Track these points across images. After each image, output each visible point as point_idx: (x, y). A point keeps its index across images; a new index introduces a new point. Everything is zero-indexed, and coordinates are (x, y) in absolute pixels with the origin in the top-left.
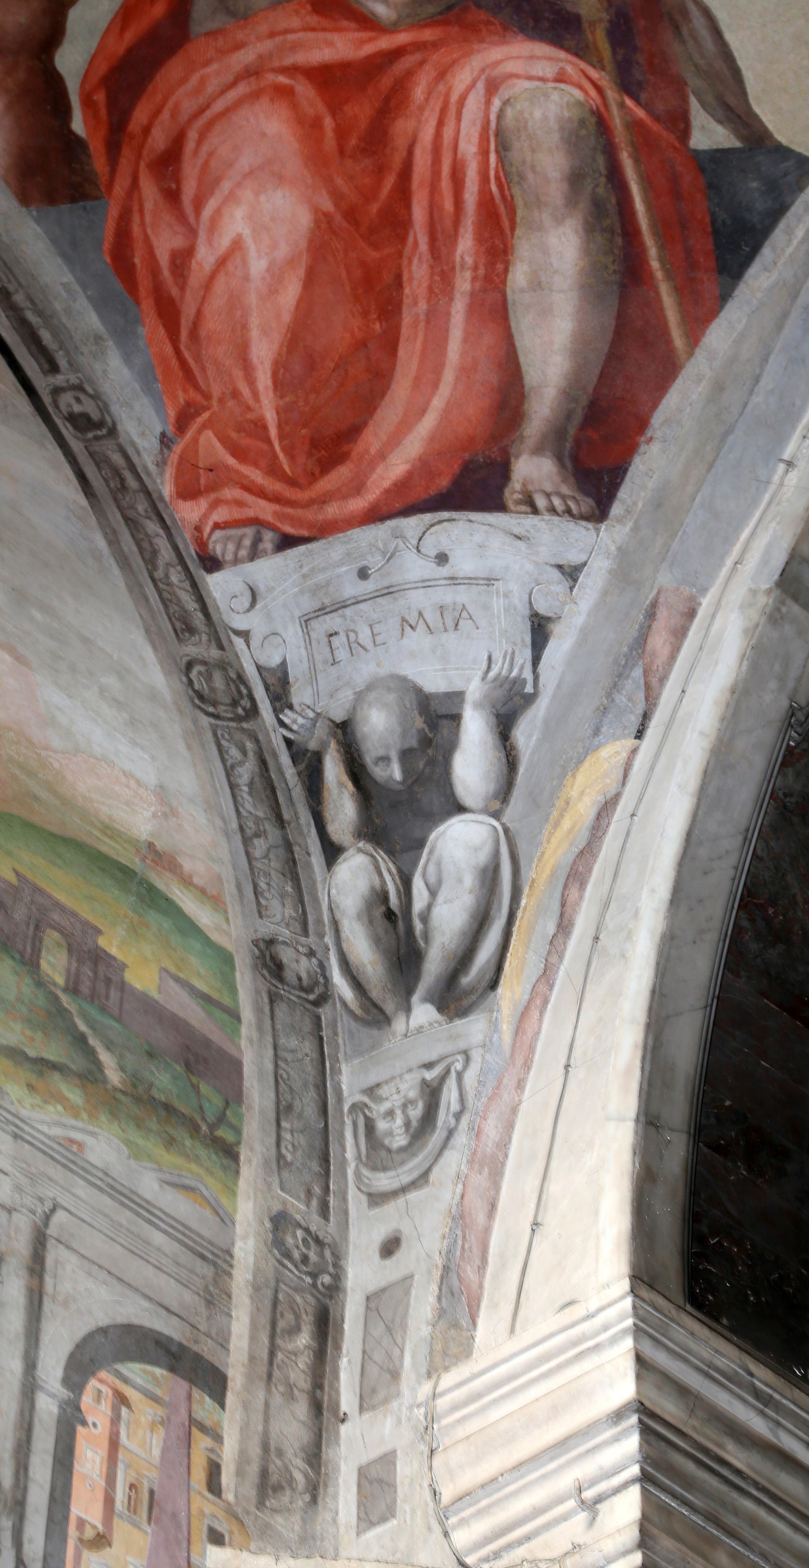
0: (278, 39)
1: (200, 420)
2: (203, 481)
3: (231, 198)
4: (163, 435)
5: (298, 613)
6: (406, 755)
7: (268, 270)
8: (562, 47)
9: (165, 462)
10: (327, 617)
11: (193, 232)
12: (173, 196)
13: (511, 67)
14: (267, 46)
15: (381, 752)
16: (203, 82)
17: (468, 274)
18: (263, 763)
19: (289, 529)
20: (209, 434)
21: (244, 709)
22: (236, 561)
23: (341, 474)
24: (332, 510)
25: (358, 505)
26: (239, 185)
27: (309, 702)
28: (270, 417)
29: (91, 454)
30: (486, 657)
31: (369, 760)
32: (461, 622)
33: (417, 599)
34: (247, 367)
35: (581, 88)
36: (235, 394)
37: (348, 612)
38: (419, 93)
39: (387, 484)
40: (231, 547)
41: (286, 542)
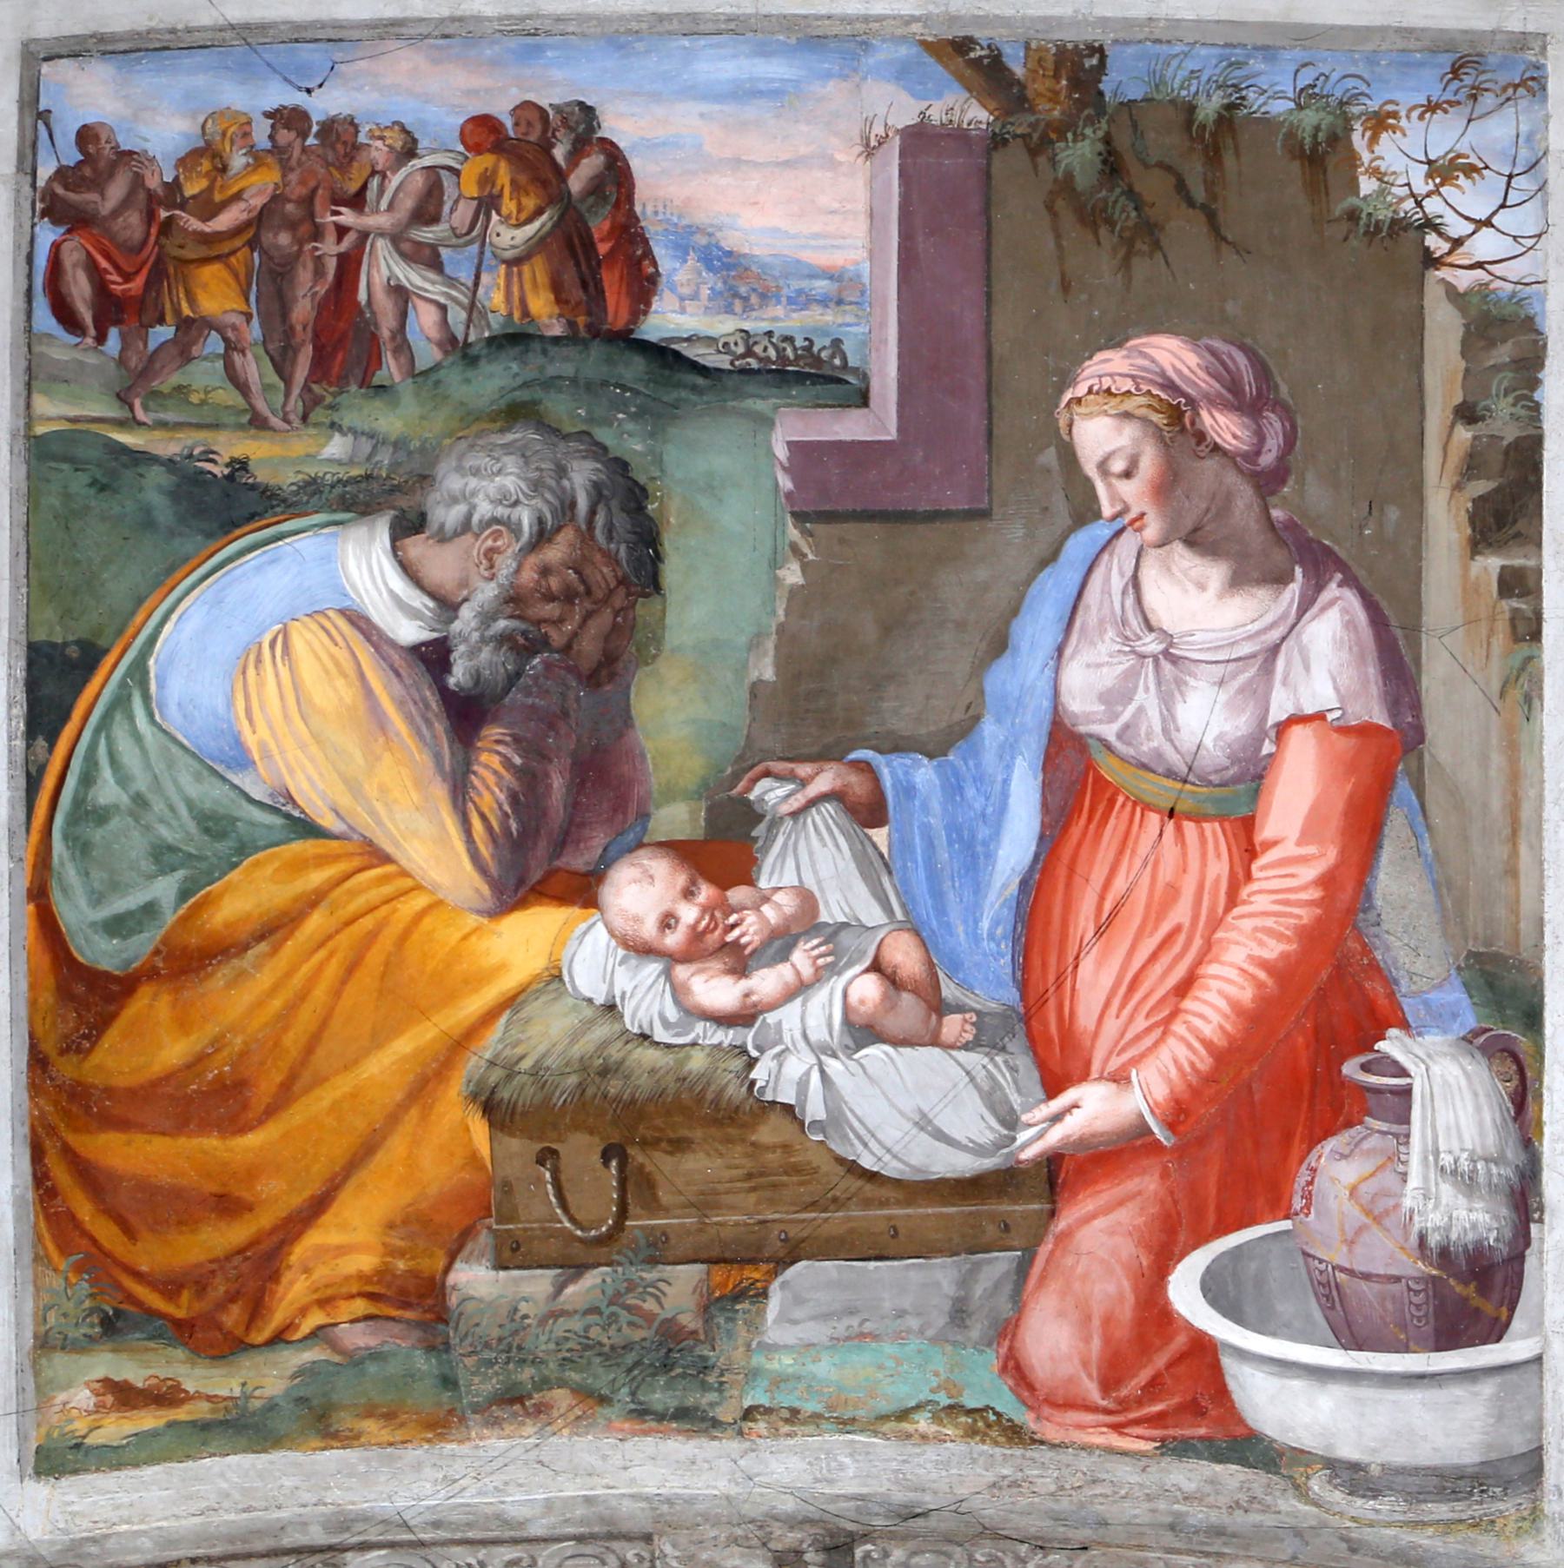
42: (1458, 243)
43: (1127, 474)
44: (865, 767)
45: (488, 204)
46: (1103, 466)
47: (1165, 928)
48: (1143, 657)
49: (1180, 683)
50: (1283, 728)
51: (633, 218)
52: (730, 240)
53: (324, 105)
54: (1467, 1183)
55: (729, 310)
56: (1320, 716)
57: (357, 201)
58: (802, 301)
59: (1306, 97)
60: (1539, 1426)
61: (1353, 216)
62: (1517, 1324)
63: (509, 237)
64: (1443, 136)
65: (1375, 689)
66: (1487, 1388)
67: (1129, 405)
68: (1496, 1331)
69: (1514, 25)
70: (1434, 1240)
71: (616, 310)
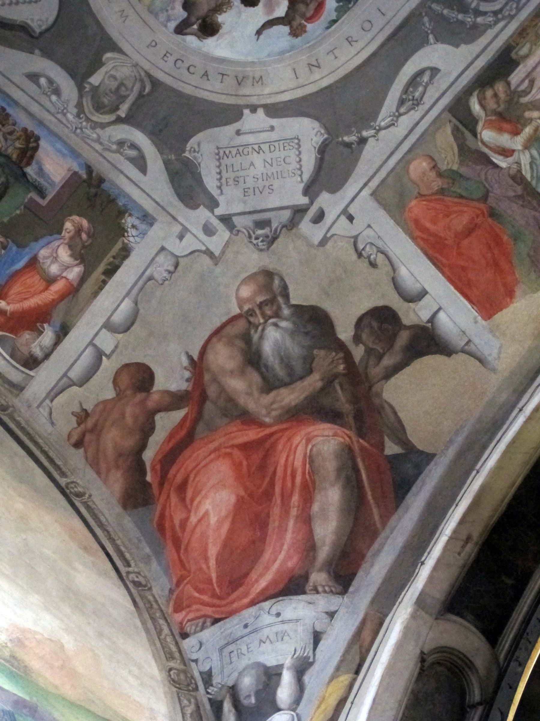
0: (228, 436)
1: (185, 581)
2: (184, 605)
3: (206, 497)
4: (170, 589)
5: (218, 647)
6: (257, 693)
7: (217, 521)
8: (336, 424)
9: (170, 599)
10: (230, 646)
11: (189, 511)
12: (183, 500)
13: (316, 433)
14: (222, 440)
15: (248, 694)
16: (198, 455)
17: (295, 509)
18: (198, 707)
19: (217, 616)
20: (189, 586)
21: (192, 688)
22: (195, 633)
23: (241, 590)
24: (235, 605)
25: (246, 601)
26: (208, 491)
27: (219, 681)
28: (214, 576)
29: (140, 595)
30: (294, 649)
31: (242, 698)
32: (284, 638)
33: (266, 631)
34: (206, 559)
35: (343, 438)
36: (201, 569)
37: (238, 642)
38: (280, 447)
39: (258, 591)
40: (193, 628)
41: (216, 621)
42: (128, 236)
43: (68, 233)
44: (8, 242)
45: (18, 139)
46: (66, 229)
47: (29, 290)
48: (52, 255)
49: (54, 263)
50: (63, 277)
51: (34, 155)
52: (43, 167)
53: (9, 110)
54: (42, 349)
55: (36, 175)
56: (68, 279)
57: (3, 125)
58: (46, 181)
59: (124, 205)
60: (27, 385)
61: (119, 223)
62: (35, 370)
63: (18, 145)
64: (137, 222)
65: (77, 282)
66: (24, 375)
67: (76, 225)
68: (31, 369)
69: (155, 216)
70: (32, 353)
71: (23, 165)
